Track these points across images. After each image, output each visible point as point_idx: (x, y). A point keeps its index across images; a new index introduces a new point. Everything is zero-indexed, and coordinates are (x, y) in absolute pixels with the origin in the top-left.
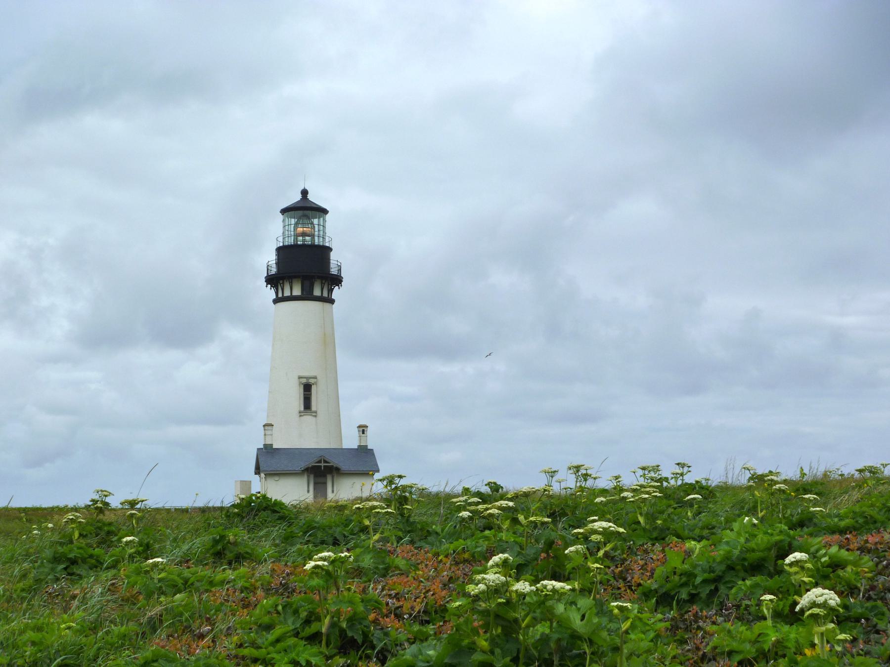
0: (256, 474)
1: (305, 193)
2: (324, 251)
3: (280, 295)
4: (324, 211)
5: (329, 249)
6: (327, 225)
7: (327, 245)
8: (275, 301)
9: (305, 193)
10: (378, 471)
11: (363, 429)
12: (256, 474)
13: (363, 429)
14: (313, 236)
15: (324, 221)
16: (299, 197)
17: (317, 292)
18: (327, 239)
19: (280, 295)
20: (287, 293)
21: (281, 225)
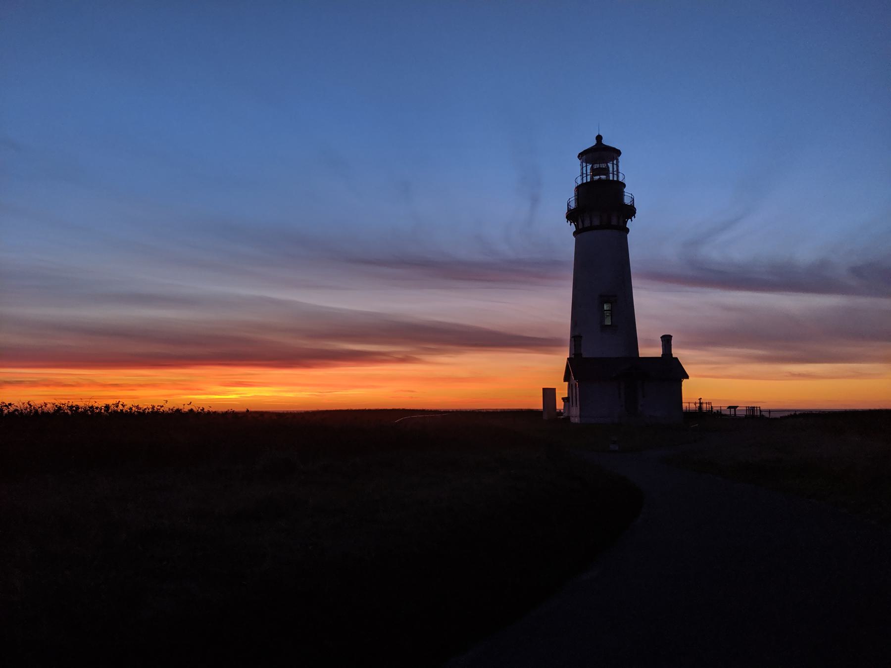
1: (599, 138)
2: (620, 186)
3: (580, 227)
4: (618, 153)
7: (620, 180)
8: (575, 234)
9: (599, 138)
10: (687, 377)
11: (667, 340)
13: (667, 340)
15: (618, 162)
16: (593, 143)
17: (614, 222)
18: (621, 175)
19: (580, 227)
20: (587, 224)
21: (579, 168)
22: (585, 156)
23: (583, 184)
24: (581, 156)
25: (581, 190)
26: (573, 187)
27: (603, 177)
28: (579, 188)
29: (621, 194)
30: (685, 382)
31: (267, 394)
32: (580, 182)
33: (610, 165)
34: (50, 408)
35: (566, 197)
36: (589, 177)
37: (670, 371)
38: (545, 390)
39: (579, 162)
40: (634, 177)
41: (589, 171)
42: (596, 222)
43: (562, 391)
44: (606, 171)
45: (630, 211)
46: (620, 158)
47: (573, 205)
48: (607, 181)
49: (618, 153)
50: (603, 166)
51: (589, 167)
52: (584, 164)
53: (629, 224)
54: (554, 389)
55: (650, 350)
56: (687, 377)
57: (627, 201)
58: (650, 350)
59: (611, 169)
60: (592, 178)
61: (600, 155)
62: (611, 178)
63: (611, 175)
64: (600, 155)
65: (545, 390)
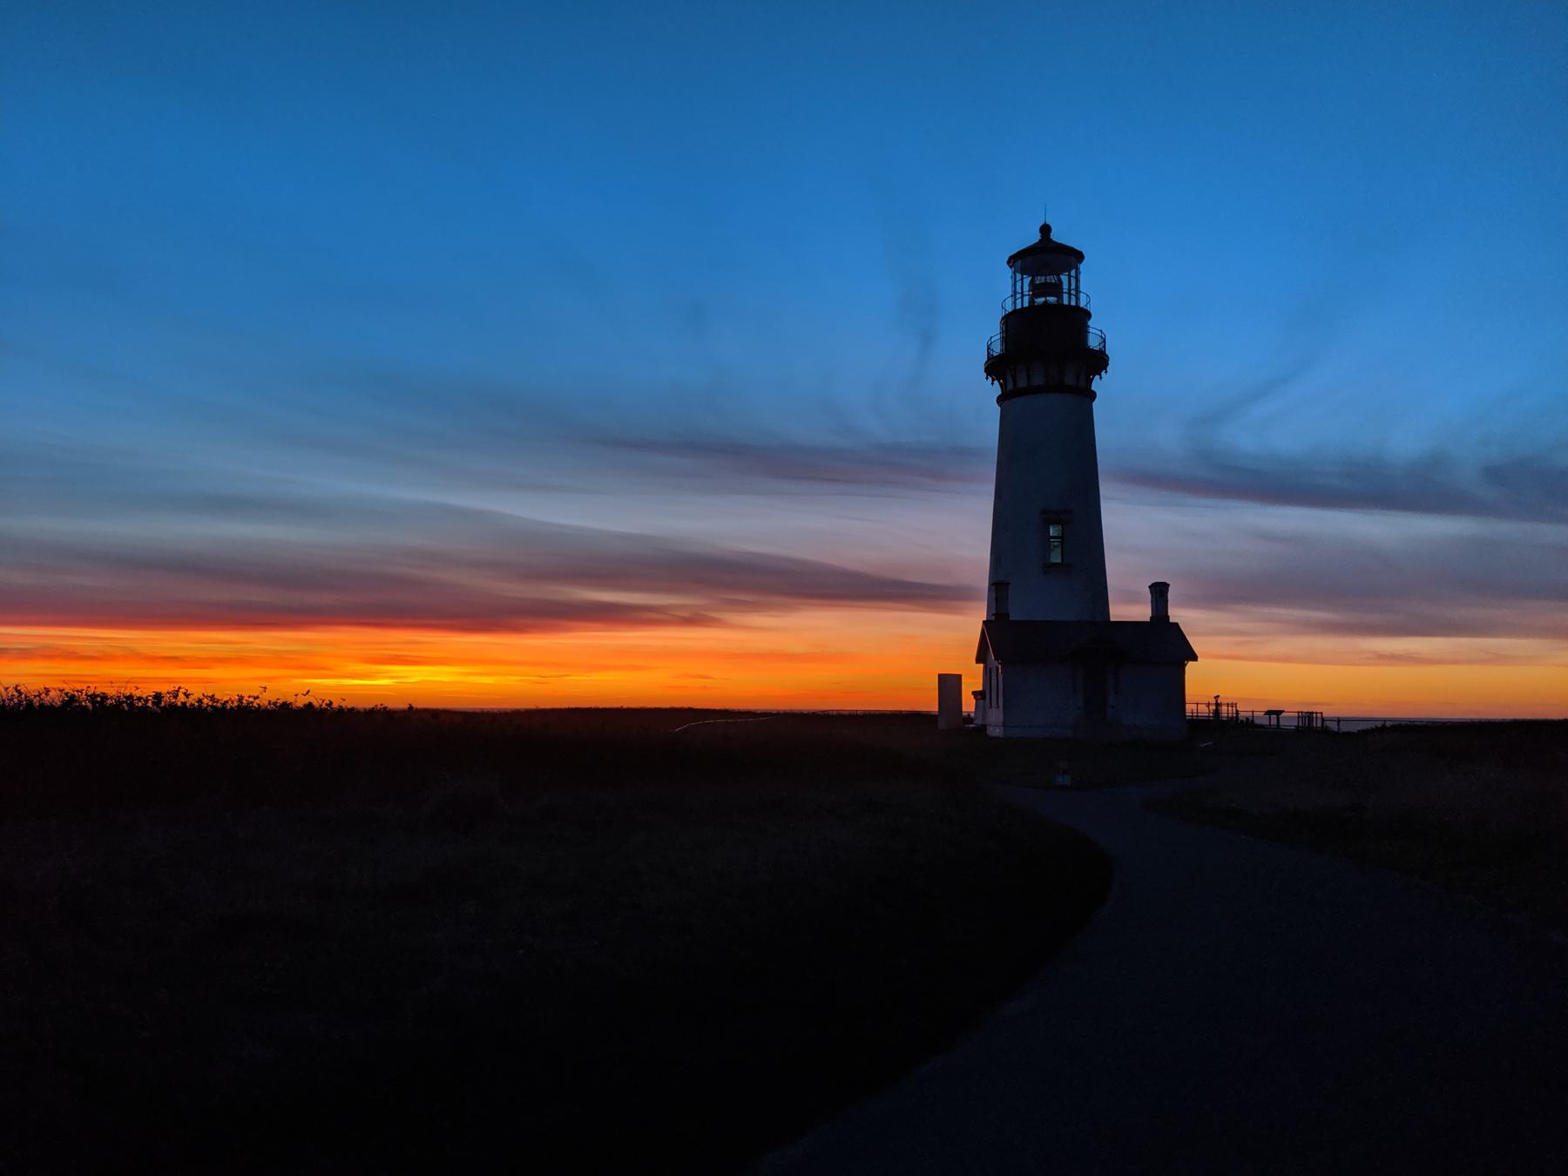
0: (978, 661)
1: (1045, 230)
3: (1010, 386)
4: (1079, 256)
5: (1088, 315)
6: (1082, 277)
8: (1000, 400)
9: (1045, 230)
10: (1195, 658)
11: (1159, 592)
12: (978, 661)
13: (1159, 592)
14: (1059, 294)
16: (1035, 237)
18: (1083, 298)
19: (1010, 386)
20: (1022, 383)
21: (1010, 282)
22: (1023, 261)
23: (1015, 312)
24: (1012, 260)
25: (1012, 322)
26: (1001, 314)
27: (1052, 299)
28: (1008, 319)
29: (1083, 331)
30: (1190, 667)
31: (446, 679)
32: (1010, 309)
33: (1064, 278)
34: (55, 697)
35: (986, 334)
36: (1026, 299)
37: (1163, 646)
38: (943, 679)
39: (1009, 272)
40: (1108, 301)
41: (1026, 288)
42: (1038, 380)
43: (973, 679)
44: (1056, 289)
45: (1098, 361)
46: (1082, 267)
47: (997, 349)
48: (1059, 306)
49: (1079, 256)
50: (1052, 279)
51: (1027, 280)
52: (1019, 276)
53: (1097, 385)
54: (959, 677)
55: (1128, 608)
56: (1195, 658)
57: (1093, 342)
58: (1128, 608)
59: (1065, 286)
60: (1031, 301)
61: (1047, 259)
62: (1066, 302)
63: (1066, 297)
64: (1047, 259)
65: (943, 679)
